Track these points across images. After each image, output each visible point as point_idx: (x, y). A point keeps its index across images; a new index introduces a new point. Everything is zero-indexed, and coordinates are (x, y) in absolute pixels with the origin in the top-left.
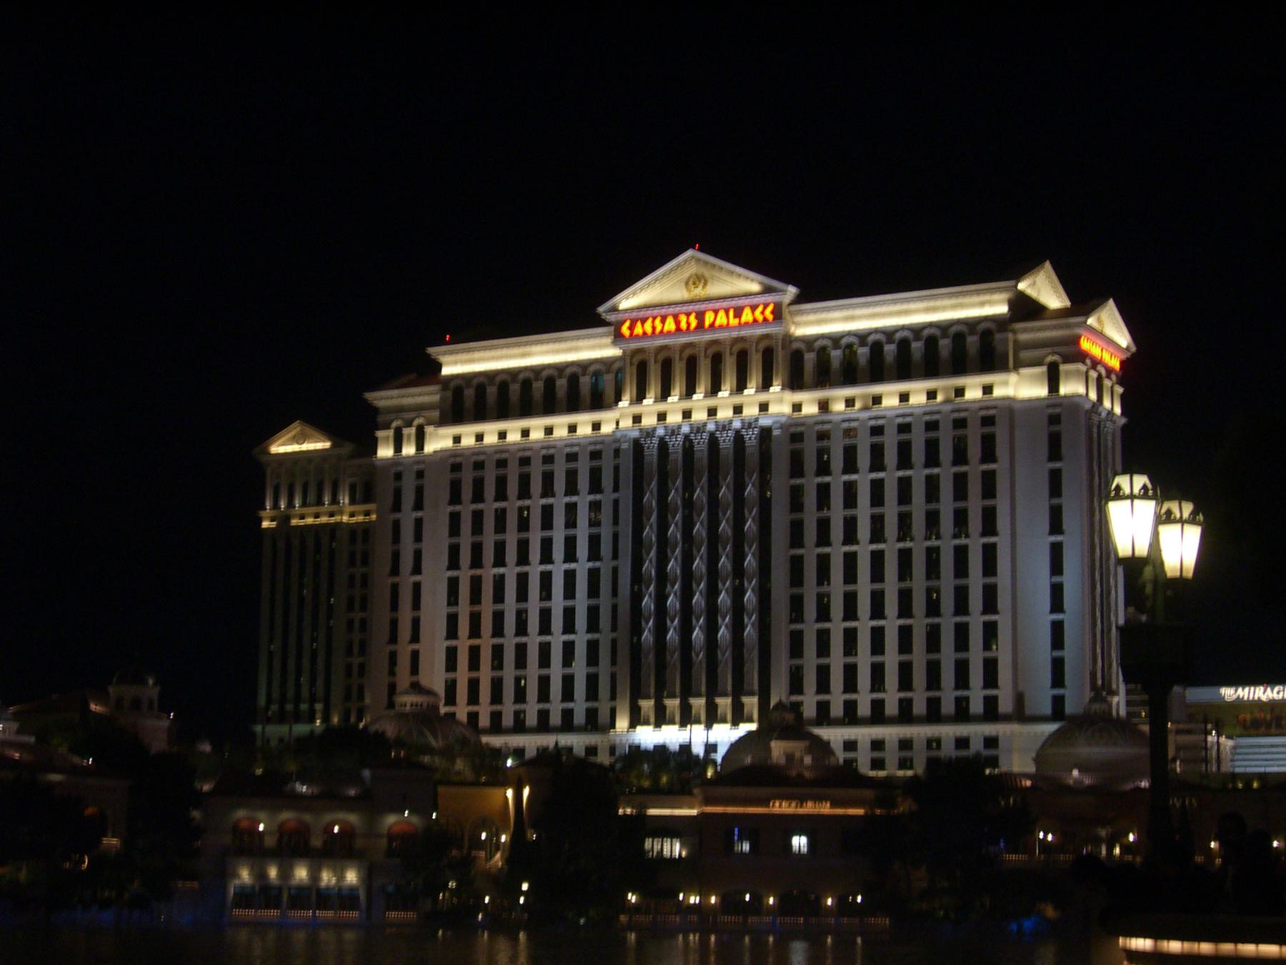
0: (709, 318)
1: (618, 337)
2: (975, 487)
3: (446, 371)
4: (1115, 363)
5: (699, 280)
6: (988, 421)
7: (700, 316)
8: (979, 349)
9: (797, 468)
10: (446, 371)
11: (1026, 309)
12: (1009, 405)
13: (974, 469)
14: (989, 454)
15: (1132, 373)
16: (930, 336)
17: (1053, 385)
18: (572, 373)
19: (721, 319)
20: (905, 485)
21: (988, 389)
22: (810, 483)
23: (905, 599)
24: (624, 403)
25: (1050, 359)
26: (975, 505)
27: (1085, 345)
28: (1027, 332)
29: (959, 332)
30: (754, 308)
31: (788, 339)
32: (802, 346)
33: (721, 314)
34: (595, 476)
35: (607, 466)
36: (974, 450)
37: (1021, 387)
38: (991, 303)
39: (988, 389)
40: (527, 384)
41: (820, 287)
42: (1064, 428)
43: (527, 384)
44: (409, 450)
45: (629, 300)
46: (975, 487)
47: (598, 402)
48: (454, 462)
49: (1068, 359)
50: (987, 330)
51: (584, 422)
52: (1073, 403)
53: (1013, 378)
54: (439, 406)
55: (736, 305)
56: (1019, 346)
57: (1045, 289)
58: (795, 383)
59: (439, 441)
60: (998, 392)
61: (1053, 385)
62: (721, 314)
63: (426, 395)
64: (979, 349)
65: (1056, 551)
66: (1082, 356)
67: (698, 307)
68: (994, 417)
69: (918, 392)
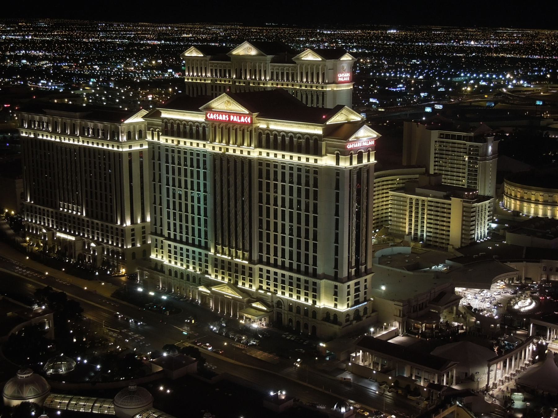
0: (232, 117)
7: (229, 117)
9: (260, 176)
17: (338, 163)
19: (235, 119)
21: (316, 161)
25: (336, 152)
30: (244, 117)
32: (261, 131)
33: (235, 117)
37: (327, 161)
38: (318, 129)
39: (316, 161)
42: (340, 177)
50: (317, 139)
53: (324, 158)
55: (240, 115)
58: (259, 145)
61: (338, 163)
62: (235, 117)
67: (229, 114)
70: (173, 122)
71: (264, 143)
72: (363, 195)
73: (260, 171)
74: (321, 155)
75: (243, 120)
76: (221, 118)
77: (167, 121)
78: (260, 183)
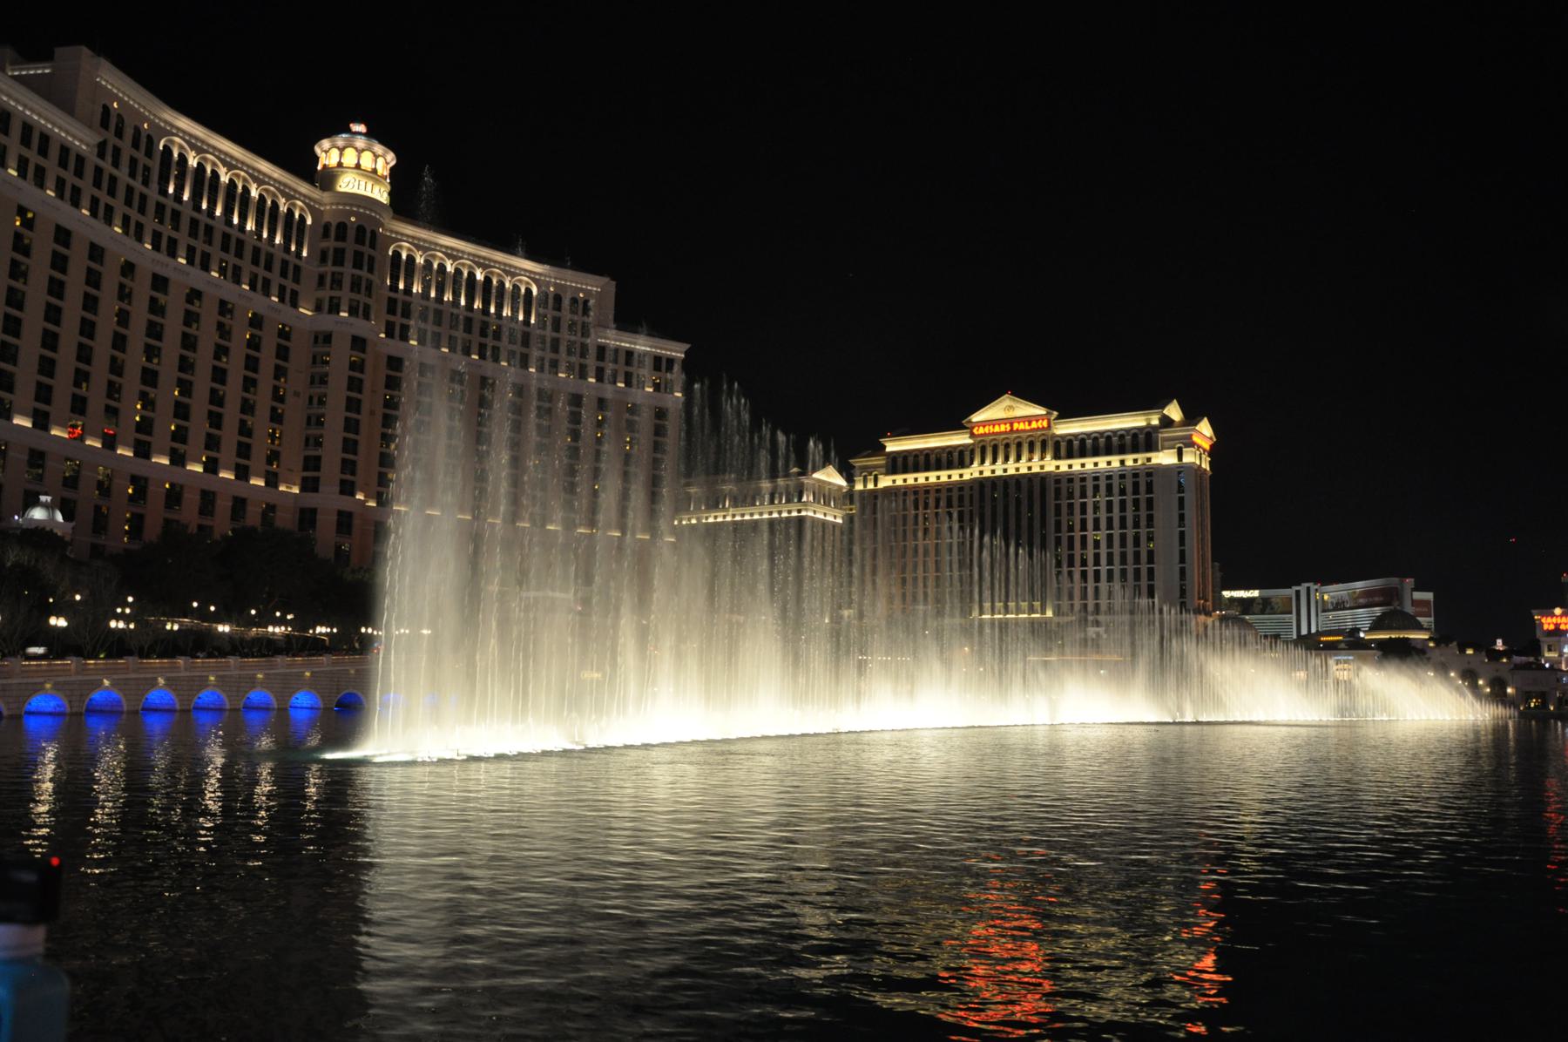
0: (1016, 426)
1: (972, 435)
2: (1143, 505)
3: (888, 449)
4: (1207, 446)
5: (1011, 407)
6: (1149, 475)
8: (1144, 441)
10: (888, 449)
11: (1167, 422)
12: (1159, 467)
13: (1143, 496)
14: (1150, 489)
15: (1213, 452)
16: (1121, 435)
17: (1180, 458)
18: (949, 451)
19: (1022, 426)
20: (1110, 504)
22: (1064, 503)
23: (1123, 556)
24: (976, 464)
26: (1143, 513)
27: (1196, 439)
28: (1166, 433)
29: (1134, 433)
31: (1054, 436)
34: (961, 499)
35: (967, 493)
36: (1143, 488)
37: (1165, 458)
40: (905, 458)
41: (1068, 412)
43: (927, 456)
44: (870, 486)
45: (977, 417)
46: (1143, 505)
47: (962, 465)
48: (890, 492)
49: (1187, 446)
51: (955, 475)
52: (1190, 466)
53: (1161, 454)
54: (886, 466)
55: (1029, 419)
56: (1165, 439)
57: (1174, 412)
58: (1057, 457)
59: (885, 482)
60: (1154, 461)
61: (1180, 458)
63: (879, 461)
64: (1144, 441)
65: (1182, 534)
66: (1192, 444)
67: (1011, 421)
68: (1152, 472)
69: (1115, 461)
70: (905, 455)
71: (1063, 451)
72: (1201, 507)
73: (1058, 492)
74: (1157, 450)
75: (1034, 425)
76: (997, 429)
77: (894, 456)
78: (1058, 507)
